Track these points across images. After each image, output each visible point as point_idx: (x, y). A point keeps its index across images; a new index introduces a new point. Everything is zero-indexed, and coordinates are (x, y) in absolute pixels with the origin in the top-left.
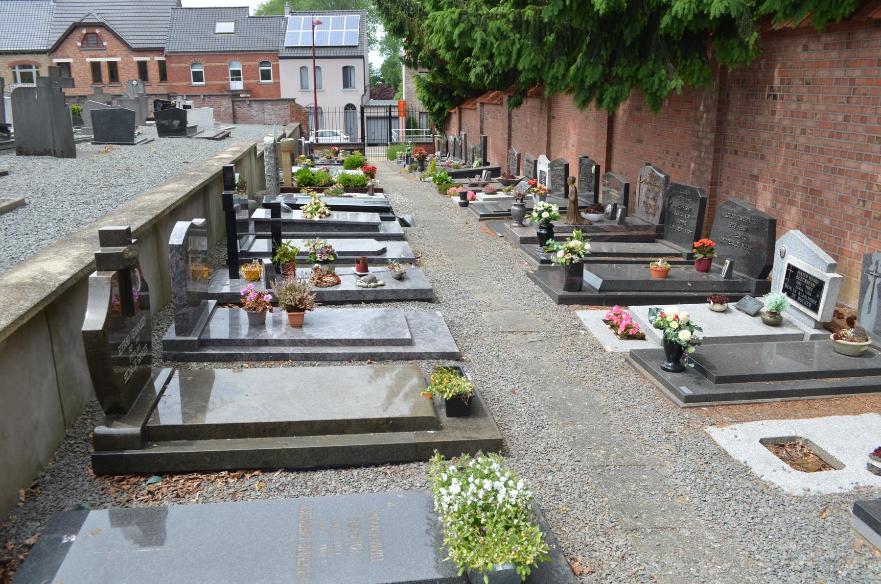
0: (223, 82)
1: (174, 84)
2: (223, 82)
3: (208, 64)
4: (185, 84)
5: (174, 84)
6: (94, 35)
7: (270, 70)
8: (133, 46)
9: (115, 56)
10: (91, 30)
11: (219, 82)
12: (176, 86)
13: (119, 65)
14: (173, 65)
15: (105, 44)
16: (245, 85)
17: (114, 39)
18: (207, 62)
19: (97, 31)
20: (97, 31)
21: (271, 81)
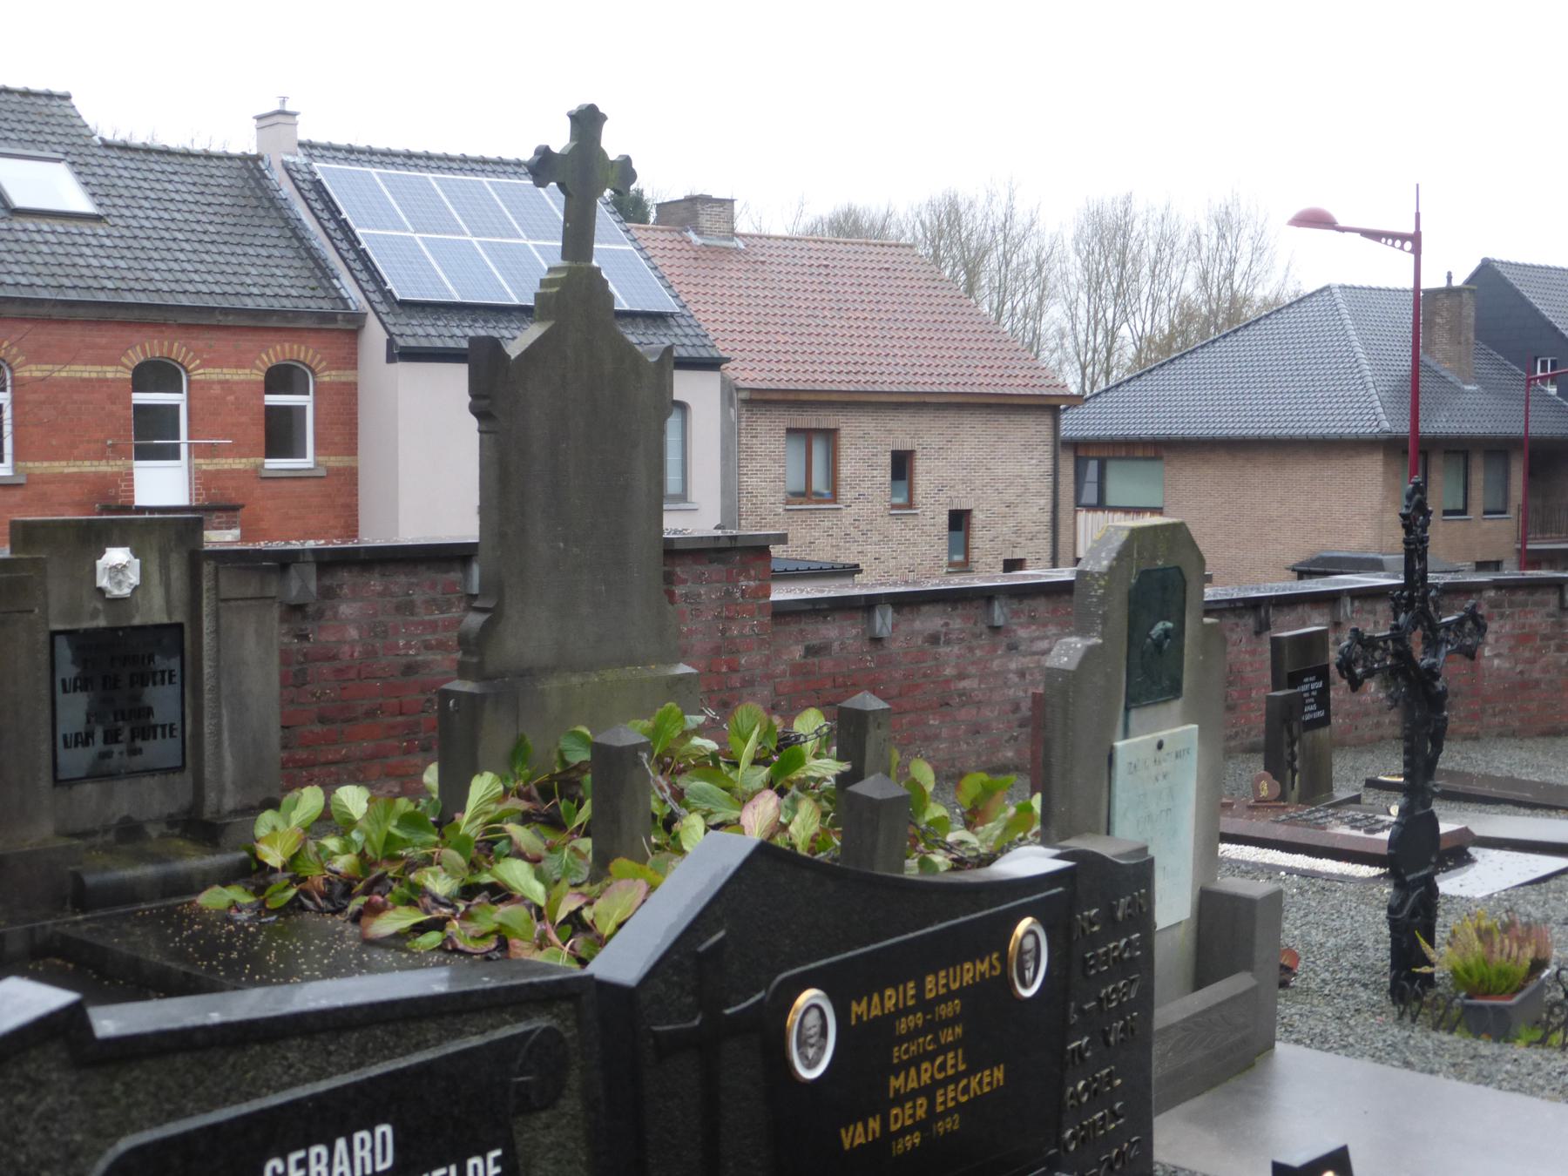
0: (104, 467)
2: (104, 467)
3: (35, 371)
7: (302, 410)
11: (88, 467)
16: (200, 480)
18: (36, 357)
21: (307, 462)
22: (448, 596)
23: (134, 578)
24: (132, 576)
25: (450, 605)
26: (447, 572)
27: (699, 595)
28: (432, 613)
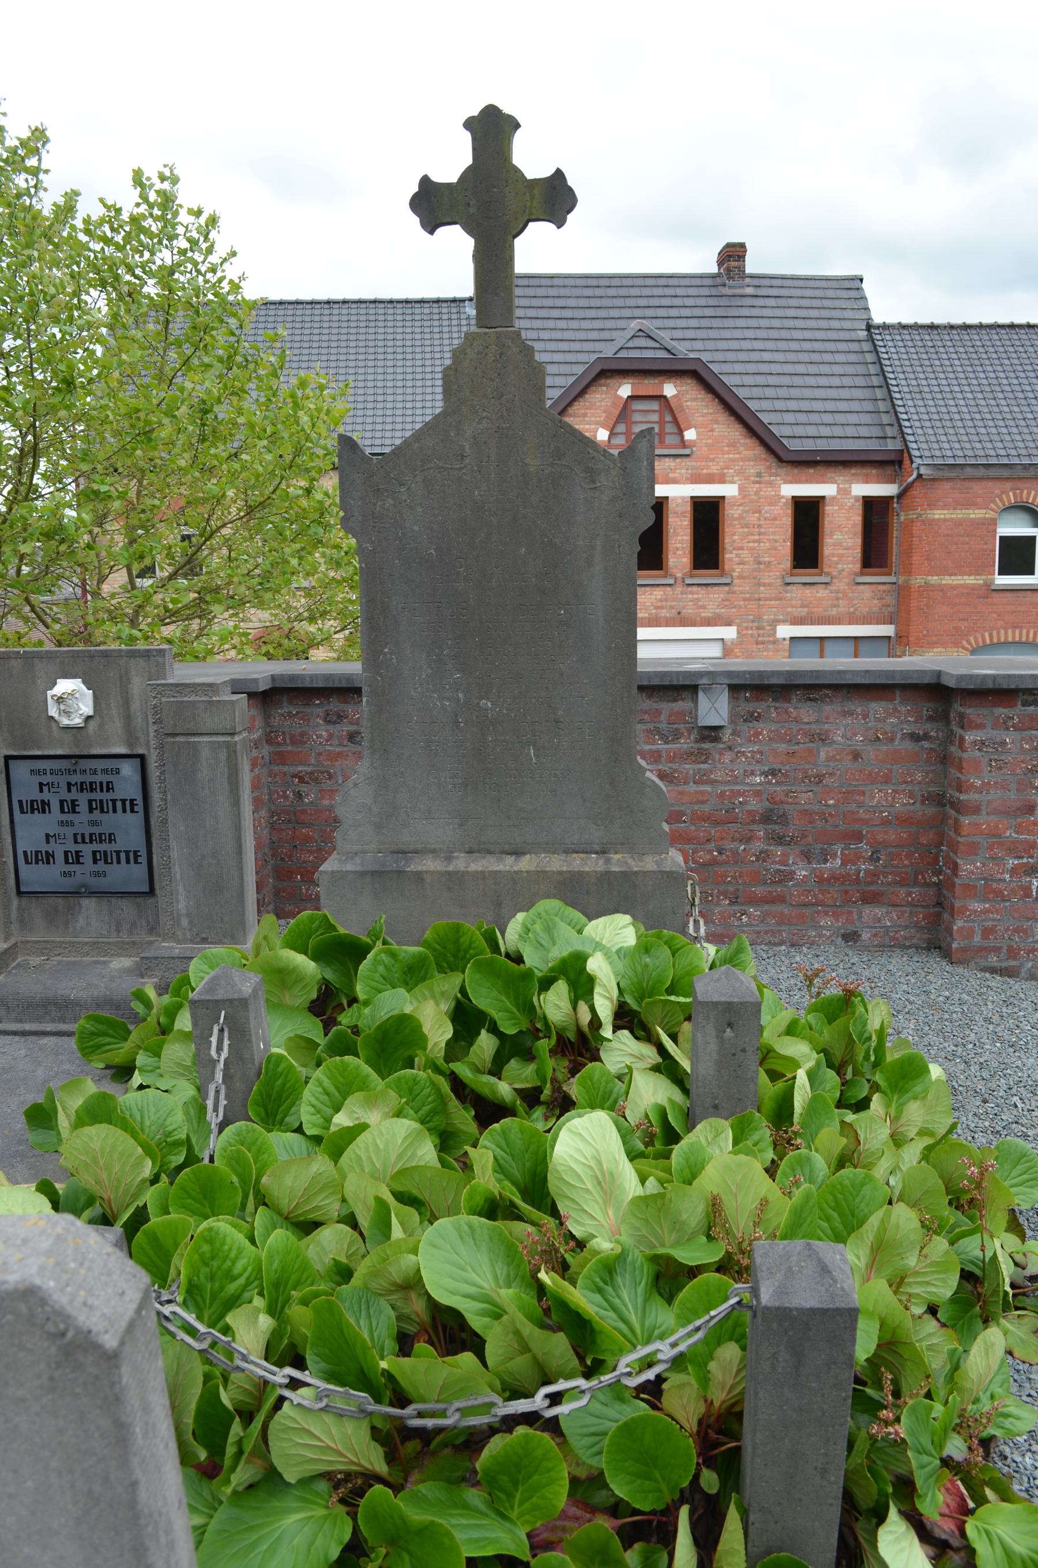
1: (934, 580)
4: (971, 580)
5: (934, 580)
6: (655, 405)
8: (793, 445)
9: (721, 479)
10: (648, 386)
12: (941, 588)
13: (730, 513)
14: (938, 514)
15: (690, 435)
17: (723, 417)
19: (669, 390)
20: (669, 390)
22: (676, 726)
23: (86, 707)
24: (82, 706)
25: (677, 735)
26: (675, 700)
27: (1003, 743)
28: (654, 743)
